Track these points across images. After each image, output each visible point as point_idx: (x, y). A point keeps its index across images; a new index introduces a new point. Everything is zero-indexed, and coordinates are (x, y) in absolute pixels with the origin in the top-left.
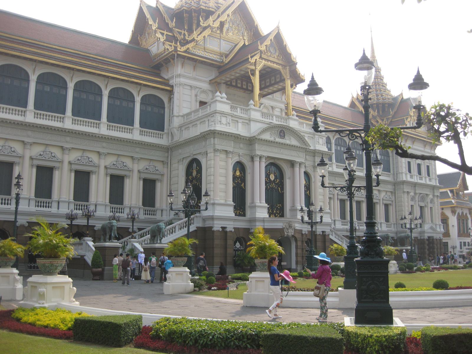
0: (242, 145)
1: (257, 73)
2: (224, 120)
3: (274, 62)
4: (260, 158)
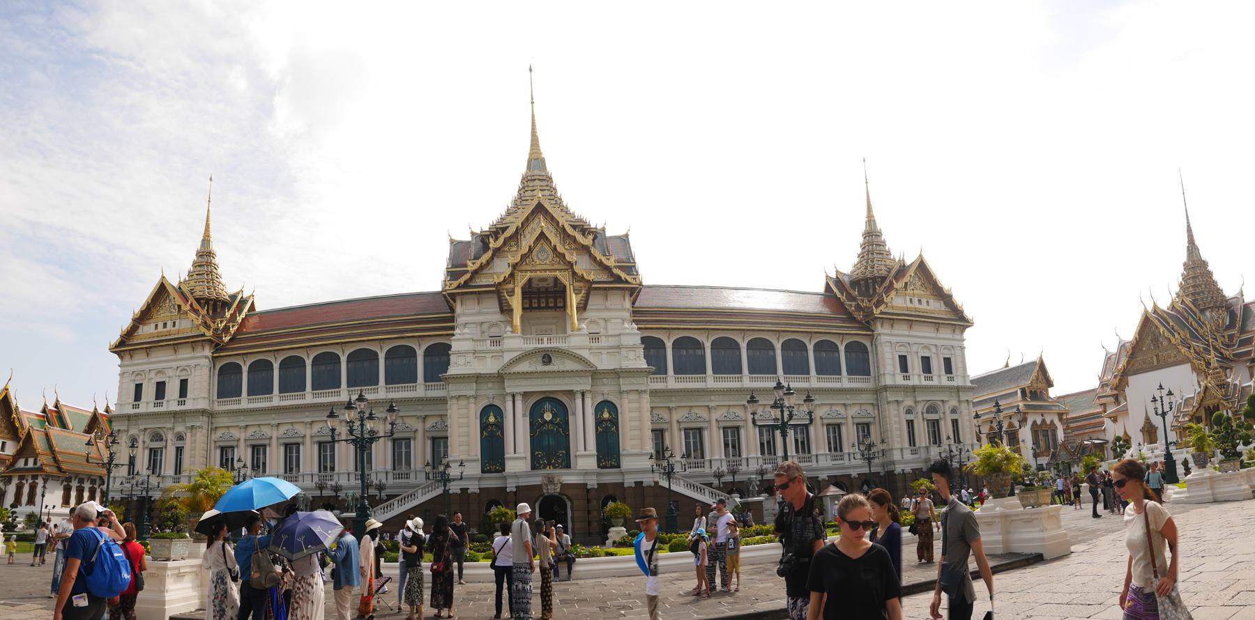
0: (490, 385)
1: (518, 291)
2: (461, 360)
4: (513, 396)
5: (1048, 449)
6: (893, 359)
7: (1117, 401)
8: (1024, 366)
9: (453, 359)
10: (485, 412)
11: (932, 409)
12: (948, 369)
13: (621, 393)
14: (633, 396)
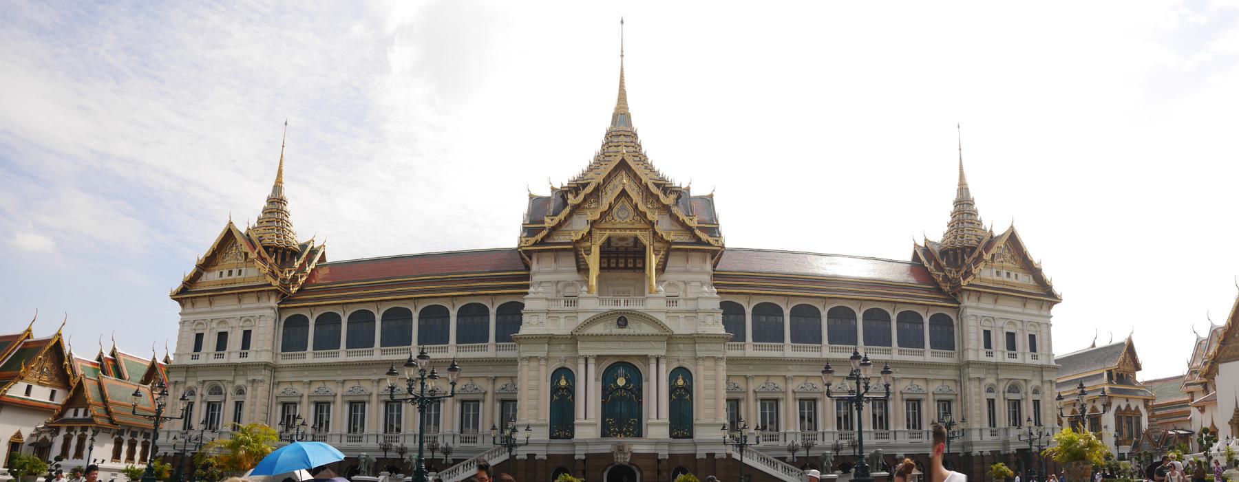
0: (563, 347)
1: (596, 250)
2: (534, 320)
3: (626, 229)
4: (586, 359)
5: (1131, 437)
6: (978, 333)
7: (1206, 390)
8: (1112, 347)
9: (525, 318)
10: (556, 375)
11: (1014, 388)
12: (1033, 348)
13: (696, 359)
14: (710, 363)
